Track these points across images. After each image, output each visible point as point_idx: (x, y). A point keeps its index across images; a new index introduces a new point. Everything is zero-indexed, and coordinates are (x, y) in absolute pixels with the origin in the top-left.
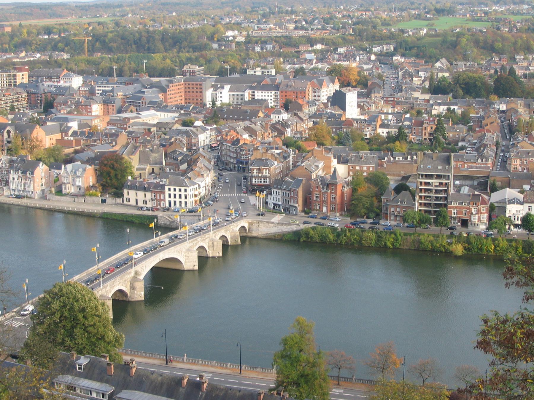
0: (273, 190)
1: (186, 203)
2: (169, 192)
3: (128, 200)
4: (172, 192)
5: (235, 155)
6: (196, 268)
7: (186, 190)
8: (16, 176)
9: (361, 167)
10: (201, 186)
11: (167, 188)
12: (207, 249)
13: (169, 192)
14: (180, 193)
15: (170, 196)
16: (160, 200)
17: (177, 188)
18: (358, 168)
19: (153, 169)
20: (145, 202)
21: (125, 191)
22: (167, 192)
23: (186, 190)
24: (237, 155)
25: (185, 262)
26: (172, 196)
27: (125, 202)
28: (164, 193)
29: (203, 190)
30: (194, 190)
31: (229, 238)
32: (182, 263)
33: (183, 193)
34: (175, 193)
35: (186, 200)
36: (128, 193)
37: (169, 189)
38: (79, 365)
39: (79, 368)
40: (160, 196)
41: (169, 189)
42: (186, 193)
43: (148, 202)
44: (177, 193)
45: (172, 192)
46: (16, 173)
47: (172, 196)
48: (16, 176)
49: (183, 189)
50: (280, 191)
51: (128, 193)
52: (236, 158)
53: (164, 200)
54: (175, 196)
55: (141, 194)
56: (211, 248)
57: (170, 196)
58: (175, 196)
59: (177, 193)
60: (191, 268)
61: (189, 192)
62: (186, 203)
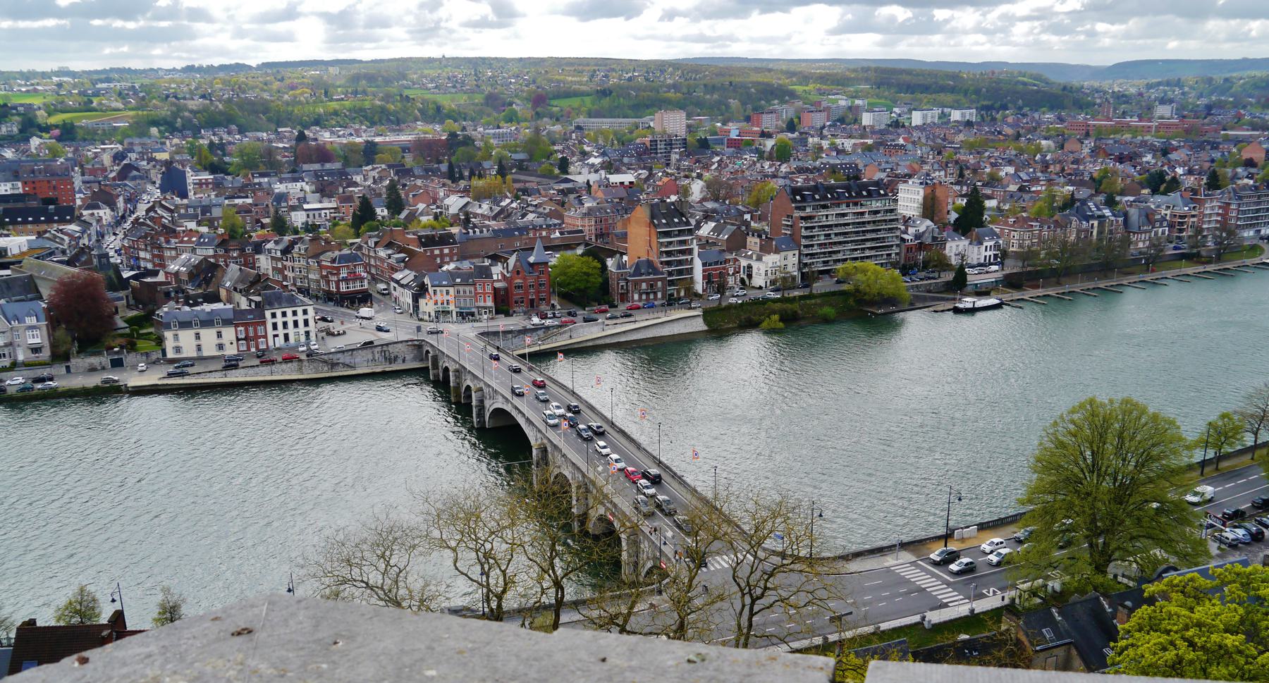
3: (178, 350)
9: (441, 250)
11: (268, 314)
15: (275, 326)
16: (256, 337)
17: (289, 311)
18: (437, 252)
20: (221, 347)
22: (270, 321)
26: (280, 326)
28: (264, 323)
33: (300, 318)
37: (274, 315)
40: (255, 331)
41: (274, 315)
43: (227, 345)
50: (451, 290)
53: (265, 337)
54: (285, 324)
55: (208, 335)
57: (275, 326)
58: (285, 324)
59: (290, 319)
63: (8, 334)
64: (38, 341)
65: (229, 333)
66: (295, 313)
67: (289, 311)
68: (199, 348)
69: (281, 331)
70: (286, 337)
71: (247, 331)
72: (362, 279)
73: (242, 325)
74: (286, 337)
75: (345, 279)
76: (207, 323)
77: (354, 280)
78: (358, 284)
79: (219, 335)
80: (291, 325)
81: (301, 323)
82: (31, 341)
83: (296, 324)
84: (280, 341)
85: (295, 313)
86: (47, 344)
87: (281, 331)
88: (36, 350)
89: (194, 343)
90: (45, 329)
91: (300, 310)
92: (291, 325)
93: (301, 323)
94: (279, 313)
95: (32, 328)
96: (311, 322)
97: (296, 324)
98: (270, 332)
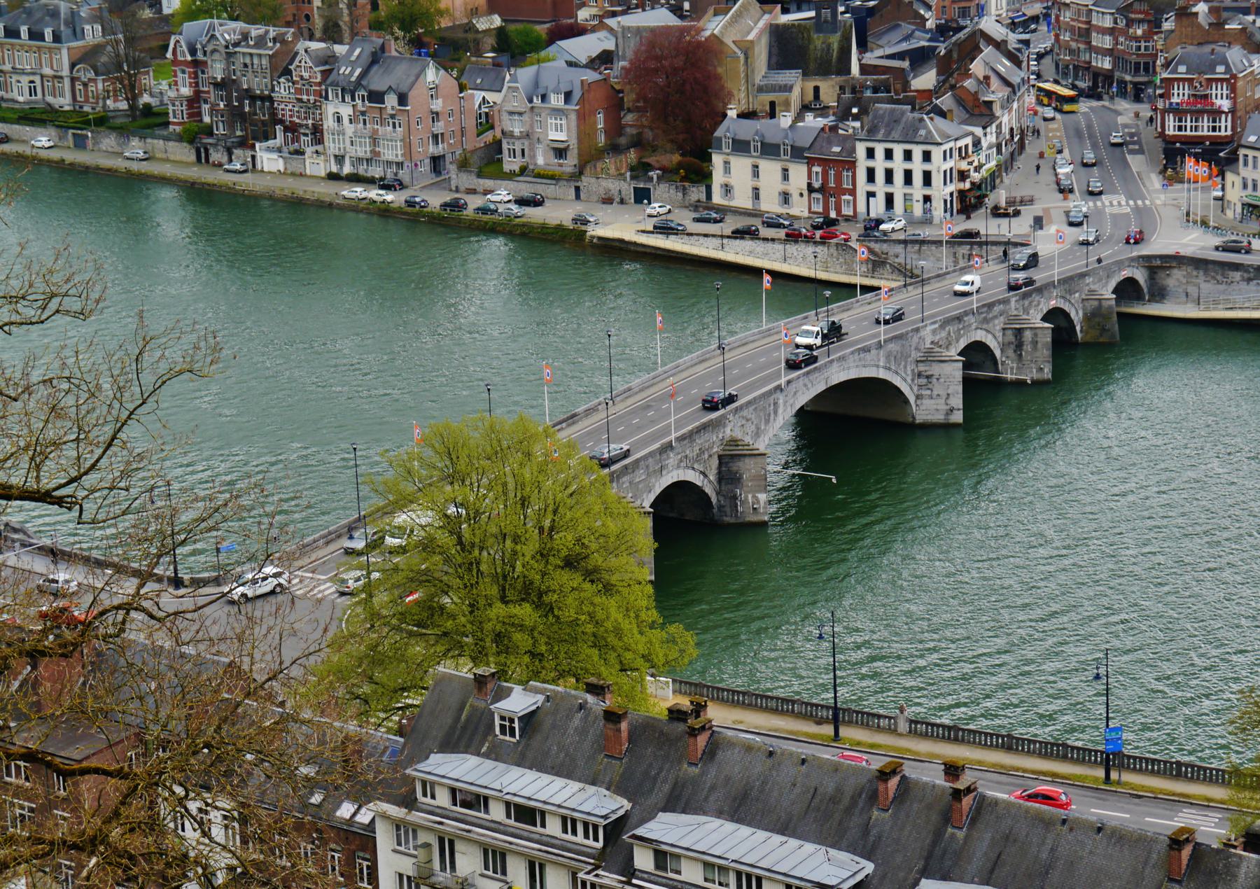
0: (1242, 152)
1: (927, 199)
2: (871, 164)
3: (727, 189)
4: (880, 164)
5: (1107, 42)
6: (958, 417)
7: (927, 157)
8: (346, 111)
10: (984, 144)
11: (861, 149)
12: (998, 353)
13: (871, 164)
14: (908, 166)
16: (840, 191)
19: (817, 89)
20: (786, 198)
21: (717, 160)
22: (862, 164)
23: (927, 157)
24: (1116, 39)
25: (918, 397)
26: (880, 176)
27: (717, 199)
28: (852, 165)
29: (988, 157)
30: (956, 154)
31: (1077, 316)
32: (906, 401)
33: (917, 166)
34: (889, 165)
35: (927, 192)
36: (727, 163)
37: (870, 153)
38: (503, 718)
39: (502, 727)
41: (870, 153)
42: (927, 167)
43: (795, 197)
44: (898, 165)
45: (880, 164)
46: (348, 98)
47: (880, 176)
48: (346, 111)
49: (917, 151)
51: (727, 163)
52: (1109, 52)
53: (853, 192)
54: (889, 175)
55: (770, 169)
56: (1010, 352)
58: (889, 175)
59: (898, 165)
60: (939, 417)
61: (939, 165)
62: (927, 199)
63: (526, 118)
64: (562, 136)
65: (799, 173)
66: (908, 156)
67: (898, 151)
68: (756, 193)
69: (880, 187)
70: (889, 199)
71: (825, 174)
72: (1216, 113)
73: (821, 162)
74: (889, 199)
75: (1178, 112)
76: (770, 150)
77: (1197, 114)
78: (1205, 123)
79: (786, 177)
80: (899, 178)
81: (918, 178)
82: (554, 135)
83: (908, 176)
84: (878, 207)
85: (908, 156)
86: (573, 143)
87: (880, 187)
88: (560, 153)
89: (749, 183)
90: (573, 117)
91: (917, 151)
92: (899, 178)
93: (918, 178)
94: (898, 151)
95: (557, 112)
96: (937, 179)
97: (908, 176)
98: (862, 186)
